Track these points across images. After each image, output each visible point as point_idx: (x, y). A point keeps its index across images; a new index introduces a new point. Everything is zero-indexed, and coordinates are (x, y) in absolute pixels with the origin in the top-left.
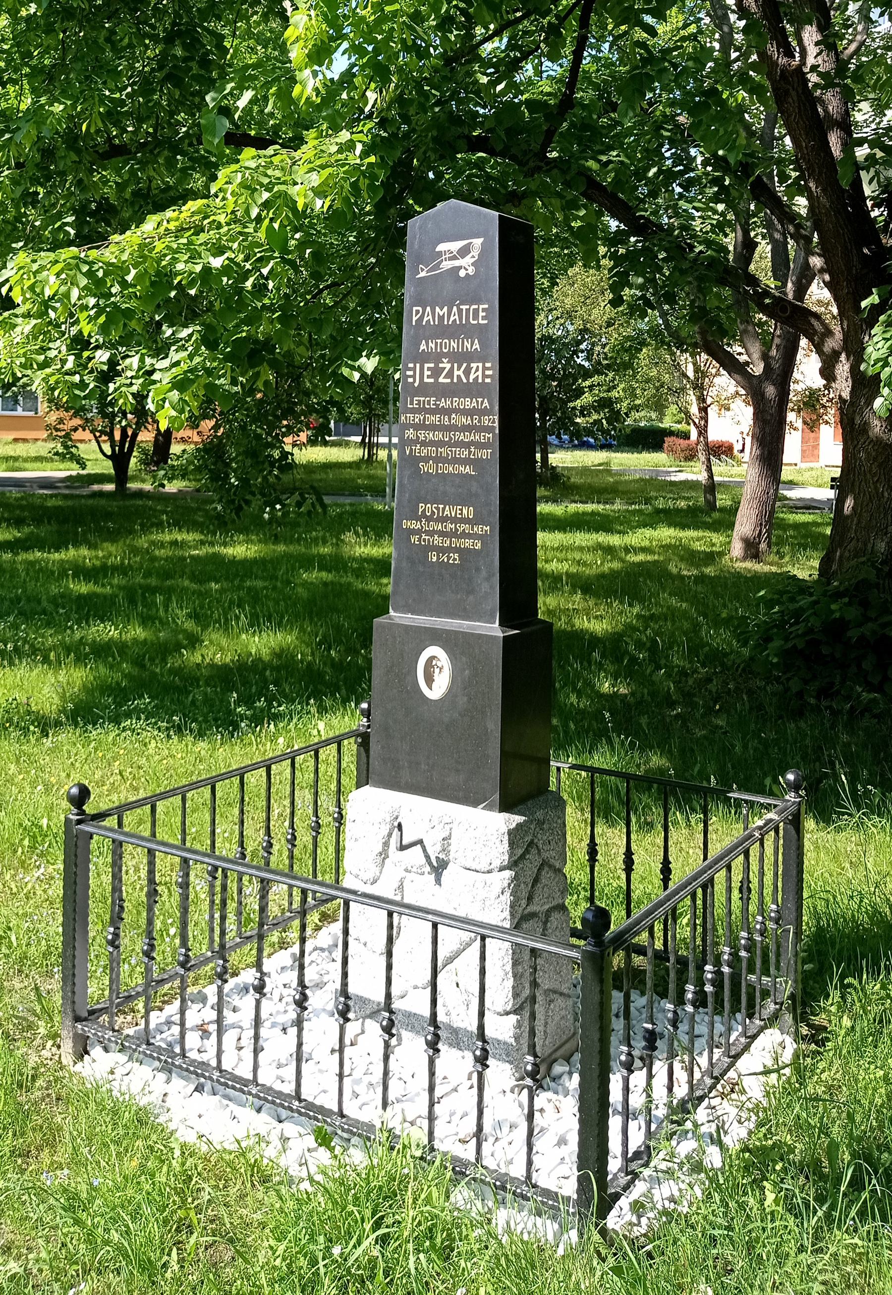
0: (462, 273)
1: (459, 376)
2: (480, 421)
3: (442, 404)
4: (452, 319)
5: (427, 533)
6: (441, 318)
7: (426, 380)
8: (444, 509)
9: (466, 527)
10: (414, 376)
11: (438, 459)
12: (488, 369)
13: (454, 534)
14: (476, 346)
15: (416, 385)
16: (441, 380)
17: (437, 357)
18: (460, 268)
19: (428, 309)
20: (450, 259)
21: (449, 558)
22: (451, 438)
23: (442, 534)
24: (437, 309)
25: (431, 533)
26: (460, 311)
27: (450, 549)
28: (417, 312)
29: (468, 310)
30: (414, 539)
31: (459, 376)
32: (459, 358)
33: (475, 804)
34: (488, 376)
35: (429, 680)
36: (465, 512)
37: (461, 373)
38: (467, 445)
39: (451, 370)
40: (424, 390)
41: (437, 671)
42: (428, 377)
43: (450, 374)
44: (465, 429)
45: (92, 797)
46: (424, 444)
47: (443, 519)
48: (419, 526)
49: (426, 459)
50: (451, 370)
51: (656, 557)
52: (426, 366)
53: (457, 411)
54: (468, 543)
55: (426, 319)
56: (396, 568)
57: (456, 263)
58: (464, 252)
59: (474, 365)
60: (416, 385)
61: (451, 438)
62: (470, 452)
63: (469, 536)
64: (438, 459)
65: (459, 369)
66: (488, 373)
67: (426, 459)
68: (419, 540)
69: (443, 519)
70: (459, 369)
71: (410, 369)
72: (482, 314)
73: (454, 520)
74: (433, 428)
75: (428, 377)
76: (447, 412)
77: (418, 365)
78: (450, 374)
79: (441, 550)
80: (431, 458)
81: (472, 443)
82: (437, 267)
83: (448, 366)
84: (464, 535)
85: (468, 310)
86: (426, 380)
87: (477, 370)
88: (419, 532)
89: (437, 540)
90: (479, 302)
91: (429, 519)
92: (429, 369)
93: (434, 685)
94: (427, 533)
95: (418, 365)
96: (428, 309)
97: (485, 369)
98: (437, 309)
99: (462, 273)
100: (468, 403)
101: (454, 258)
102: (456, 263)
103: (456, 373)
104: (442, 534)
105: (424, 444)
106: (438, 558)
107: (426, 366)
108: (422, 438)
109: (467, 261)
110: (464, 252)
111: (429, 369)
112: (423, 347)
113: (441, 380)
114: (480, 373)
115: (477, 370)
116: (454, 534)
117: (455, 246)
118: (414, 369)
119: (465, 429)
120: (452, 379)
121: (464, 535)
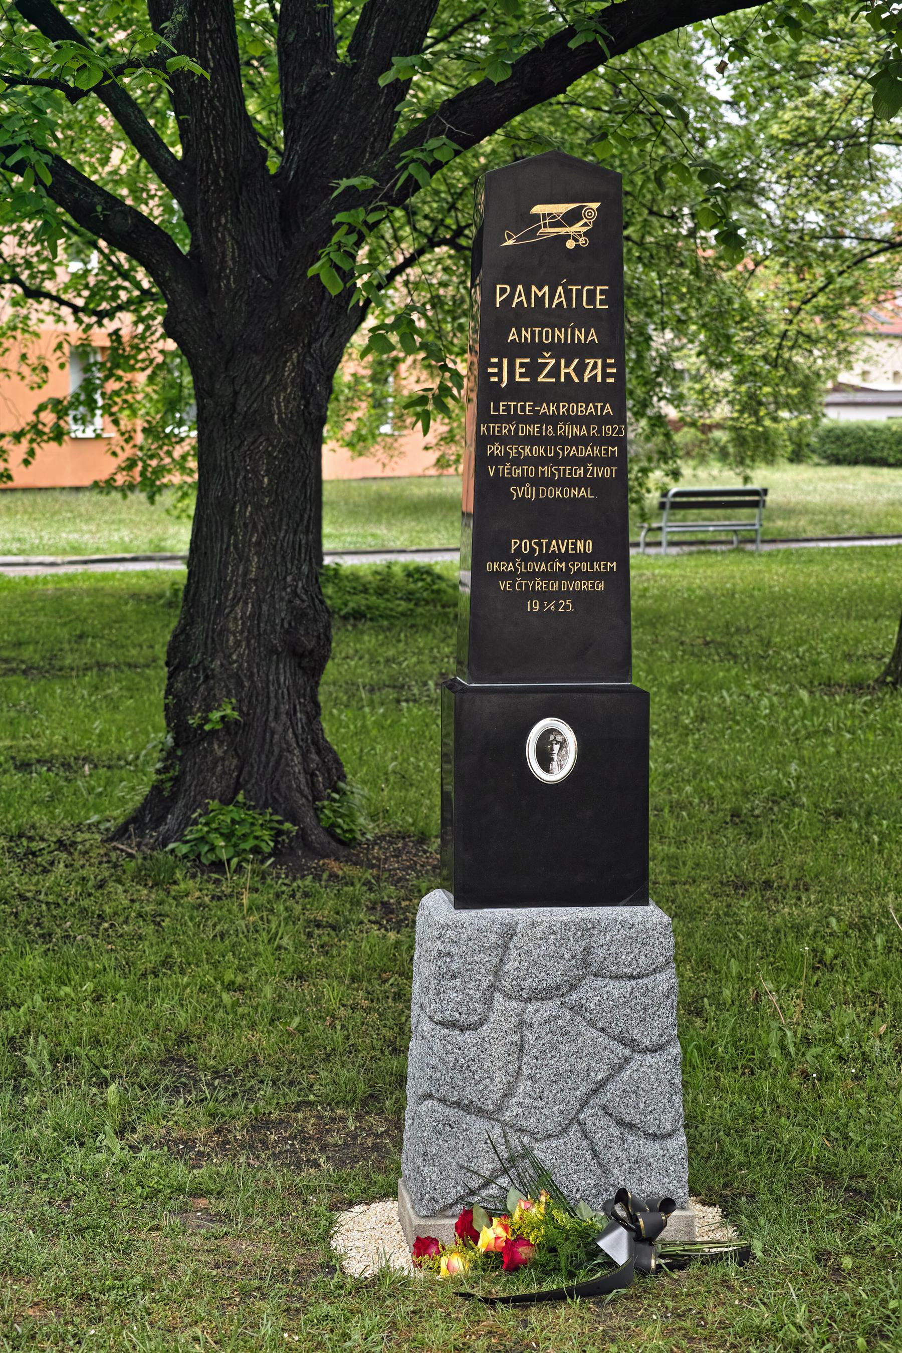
0: (570, 244)
1: (567, 375)
2: (599, 431)
3: (544, 409)
4: (556, 302)
6: (540, 300)
7: (518, 379)
8: (548, 545)
9: (585, 567)
10: (499, 374)
12: (611, 366)
14: (593, 336)
17: (534, 350)
18: (567, 237)
19: (520, 287)
20: (553, 225)
21: (557, 606)
23: (544, 576)
24: (534, 288)
25: (532, 576)
26: (568, 293)
27: (560, 595)
28: (503, 291)
29: (579, 293)
31: (567, 375)
34: (611, 375)
35: (545, 760)
36: (580, 546)
37: (570, 370)
39: (557, 366)
40: (515, 391)
42: (522, 375)
46: (517, 462)
49: (520, 482)
50: (557, 366)
52: (518, 361)
54: (585, 585)
57: (562, 231)
58: (572, 218)
62: (586, 471)
63: (586, 576)
65: (567, 366)
67: (520, 482)
68: (512, 586)
69: (549, 557)
70: (567, 366)
71: (493, 365)
72: (599, 297)
73: (565, 557)
74: (530, 440)
75: (522, 375)
76: (553, 420)
77: (505, 361)
80: (528, 479)
81: (589, 459)
82: (533, 234)
85: (579, 293)
86: (518, 379)
87: (595, 366)
88: (512, 576)
89: (539, 585)
91: (527, 558)
92: (522, 365)
93: (554, 765)
95: (505, 361)
96: (520, 287)
97: (605, 366)
98: (534, 288)
99: (570, 244)
100: (581, 409)
102: (562, 231)
103: (563, 371)
104: (544, 576)
105: (517, 462)
106: (542, 606)
107: (518, 361)
109: (578, 228)
110: (572, 218)
111: (522, 365)
112: (512, 336)
113: (540, 379)
114: (599, 371)
115: (595, 366)
116: (565, 575)
117: (562, 209)
118: (499, 365)
121: (580, 575)
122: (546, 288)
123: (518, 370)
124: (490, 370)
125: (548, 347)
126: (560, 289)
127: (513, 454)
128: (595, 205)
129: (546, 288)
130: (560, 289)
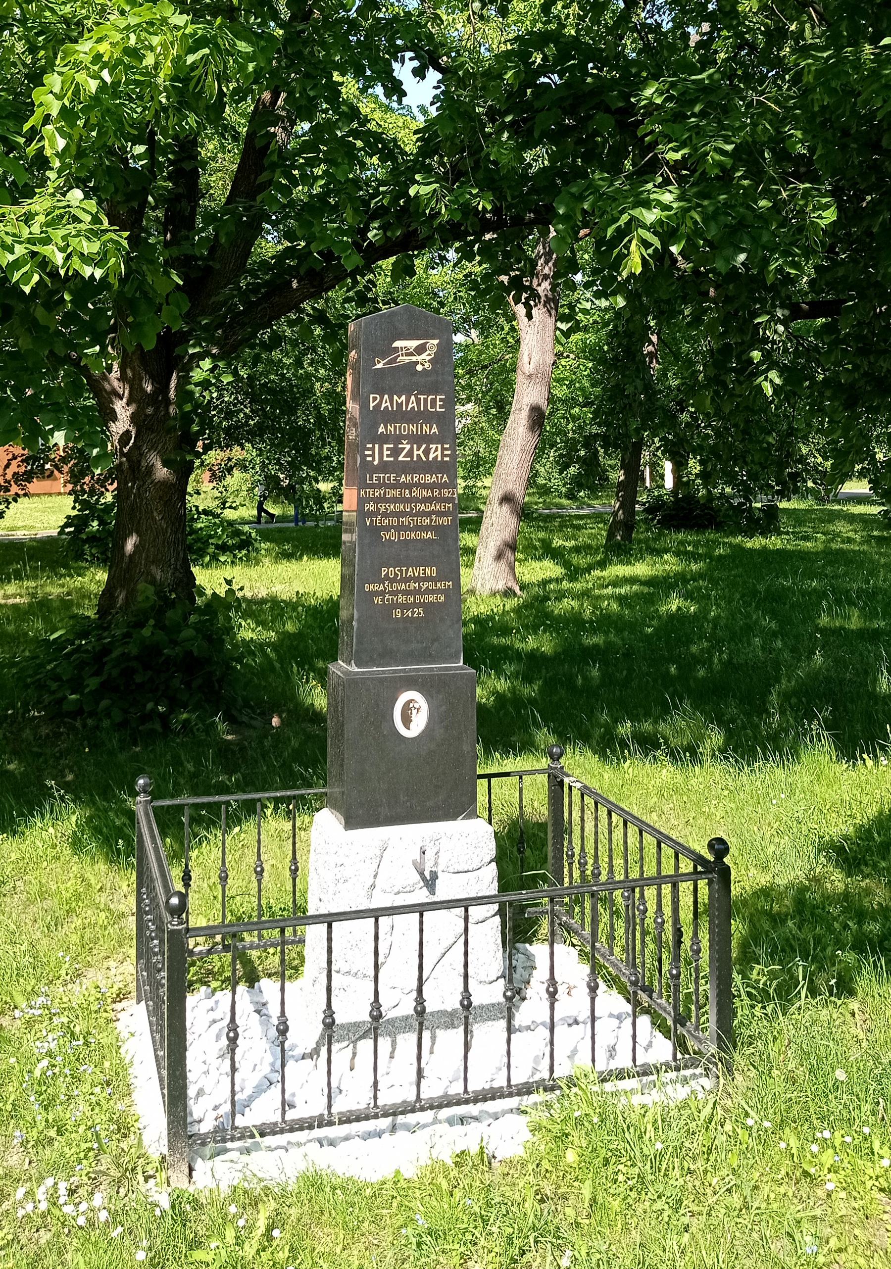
0: (419, 368)
1: (418, 455)
2: (440, 494)
3: (403, 479)
4: (410, 406)
5: (391, 593)
6: (400, 405)
7: (385, 459)
8: (407, 571)
9: (430, 585)
10: (373, 456)
11: (400, 528)
12: (447, 449)
13: (418, 592)
14: (435, 430)
15: (376, 463)
16: (400, 458)
17: (398, 439)
18: (417, 363)
19: (386, 396)
20: (407, 355)
21: (413, 613)
22: (412, 509)
23: (405, 593)
24: (395, 397)
25: (395, 593)
26: (418, 401)
27: (415, 605)
28: (375, 399)
29: (426, 400)
30: (377, 600)
31: (418, 455)
32: (418, 439)
33: (453, 817)
34: (447, 456)
35: (407, 721)
36: (428, 571)
37: (420, 452)
38: (429, 514)
39: (412, 449)
40: (384, 467)
41: (414, 712)
42: (388, 456)
43: (410, 454)
44: (425, 500)
45: (725, 837)
46: (385, 515)
47: (407, 580)
48: (382, 588)
49: (387, 529)
50: (412, 449)
51: (726, 540)
52: (385, 446)
53: (418, 485)
54: (432, 598)
55: (383, 405)
56: (358, 628)
57: (414, 359)
58: (420, 350)
59: (433, 446)
60: (376, 463)
61: (412, 509)
62: (431, 520)
63: (433, 592)
64: (400, 528)
65: (418, 450)
66: (446, 452)
67: (387, 529)
68: (383, 600)
69: (407, 580)
70: (418, 450)
71: (368, 449)
72: (438, 403)
73: (417, 579)
74: (394, 500)
75: (388, 456)
76: (410, 486)
77: (377, 446)
78: (410, 454)
79: (405, 607)
80: (393, 527)
81: (433, 512)
82: (394, 360)
83: (408, 447)
84: (428, 591)
85: (426, 400)
86: (385, 459)
87: (436, 450)
88: (382, 593)
89: (401, 599)
90: (436, 393)
91: (392, 581)
92: (388, 449)
93: (412, 725)
94: (391, 593)
95: (377, 446)
96: (386, 396)
97: (443, 449)
98: (395, 397)
99: (419, 368)
100: (429, 479)
101: (411, 354)
102: (414, 359)
103: (416, 453)
104: (405, 593)
105: (385, 515)
106: (403, 614)
107: (385, 446)
108: (383, 509)
109: (424, 356)
110: (420, 350)
111: (388, 449)
112: (381, 429)
113: (400, 458)
114: (439, 452)
115: (436, 450)
116: (418, 592)
117: (413, 344)
118: (373, 449)
119: (425, 500)
120: (412, 457)
121: (428, 591)
122: (403, 397)
123: (386, 453)
124: (367, 453)
125: (404, 437)
126: (413, 398)
127: (383, 509)
128: (436, 342)
129: (403, 397)
130: (413, 398)
